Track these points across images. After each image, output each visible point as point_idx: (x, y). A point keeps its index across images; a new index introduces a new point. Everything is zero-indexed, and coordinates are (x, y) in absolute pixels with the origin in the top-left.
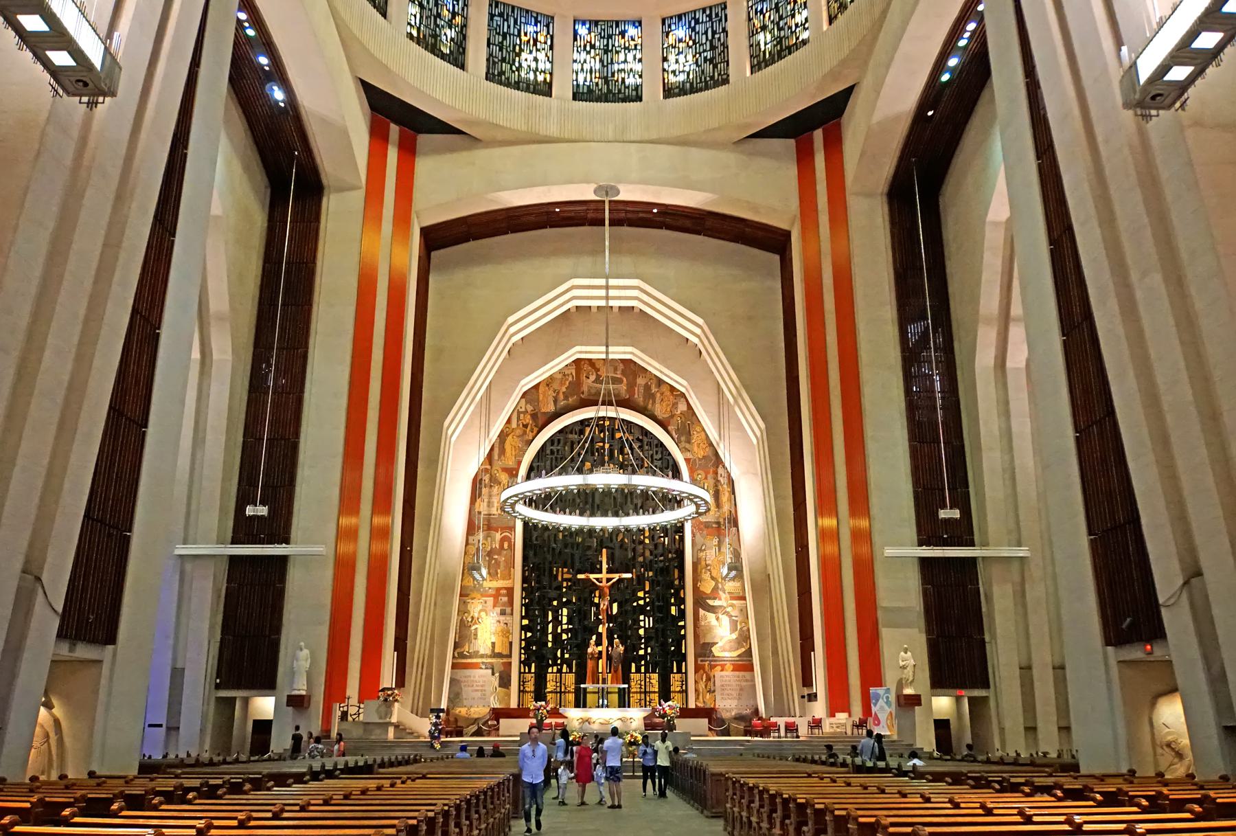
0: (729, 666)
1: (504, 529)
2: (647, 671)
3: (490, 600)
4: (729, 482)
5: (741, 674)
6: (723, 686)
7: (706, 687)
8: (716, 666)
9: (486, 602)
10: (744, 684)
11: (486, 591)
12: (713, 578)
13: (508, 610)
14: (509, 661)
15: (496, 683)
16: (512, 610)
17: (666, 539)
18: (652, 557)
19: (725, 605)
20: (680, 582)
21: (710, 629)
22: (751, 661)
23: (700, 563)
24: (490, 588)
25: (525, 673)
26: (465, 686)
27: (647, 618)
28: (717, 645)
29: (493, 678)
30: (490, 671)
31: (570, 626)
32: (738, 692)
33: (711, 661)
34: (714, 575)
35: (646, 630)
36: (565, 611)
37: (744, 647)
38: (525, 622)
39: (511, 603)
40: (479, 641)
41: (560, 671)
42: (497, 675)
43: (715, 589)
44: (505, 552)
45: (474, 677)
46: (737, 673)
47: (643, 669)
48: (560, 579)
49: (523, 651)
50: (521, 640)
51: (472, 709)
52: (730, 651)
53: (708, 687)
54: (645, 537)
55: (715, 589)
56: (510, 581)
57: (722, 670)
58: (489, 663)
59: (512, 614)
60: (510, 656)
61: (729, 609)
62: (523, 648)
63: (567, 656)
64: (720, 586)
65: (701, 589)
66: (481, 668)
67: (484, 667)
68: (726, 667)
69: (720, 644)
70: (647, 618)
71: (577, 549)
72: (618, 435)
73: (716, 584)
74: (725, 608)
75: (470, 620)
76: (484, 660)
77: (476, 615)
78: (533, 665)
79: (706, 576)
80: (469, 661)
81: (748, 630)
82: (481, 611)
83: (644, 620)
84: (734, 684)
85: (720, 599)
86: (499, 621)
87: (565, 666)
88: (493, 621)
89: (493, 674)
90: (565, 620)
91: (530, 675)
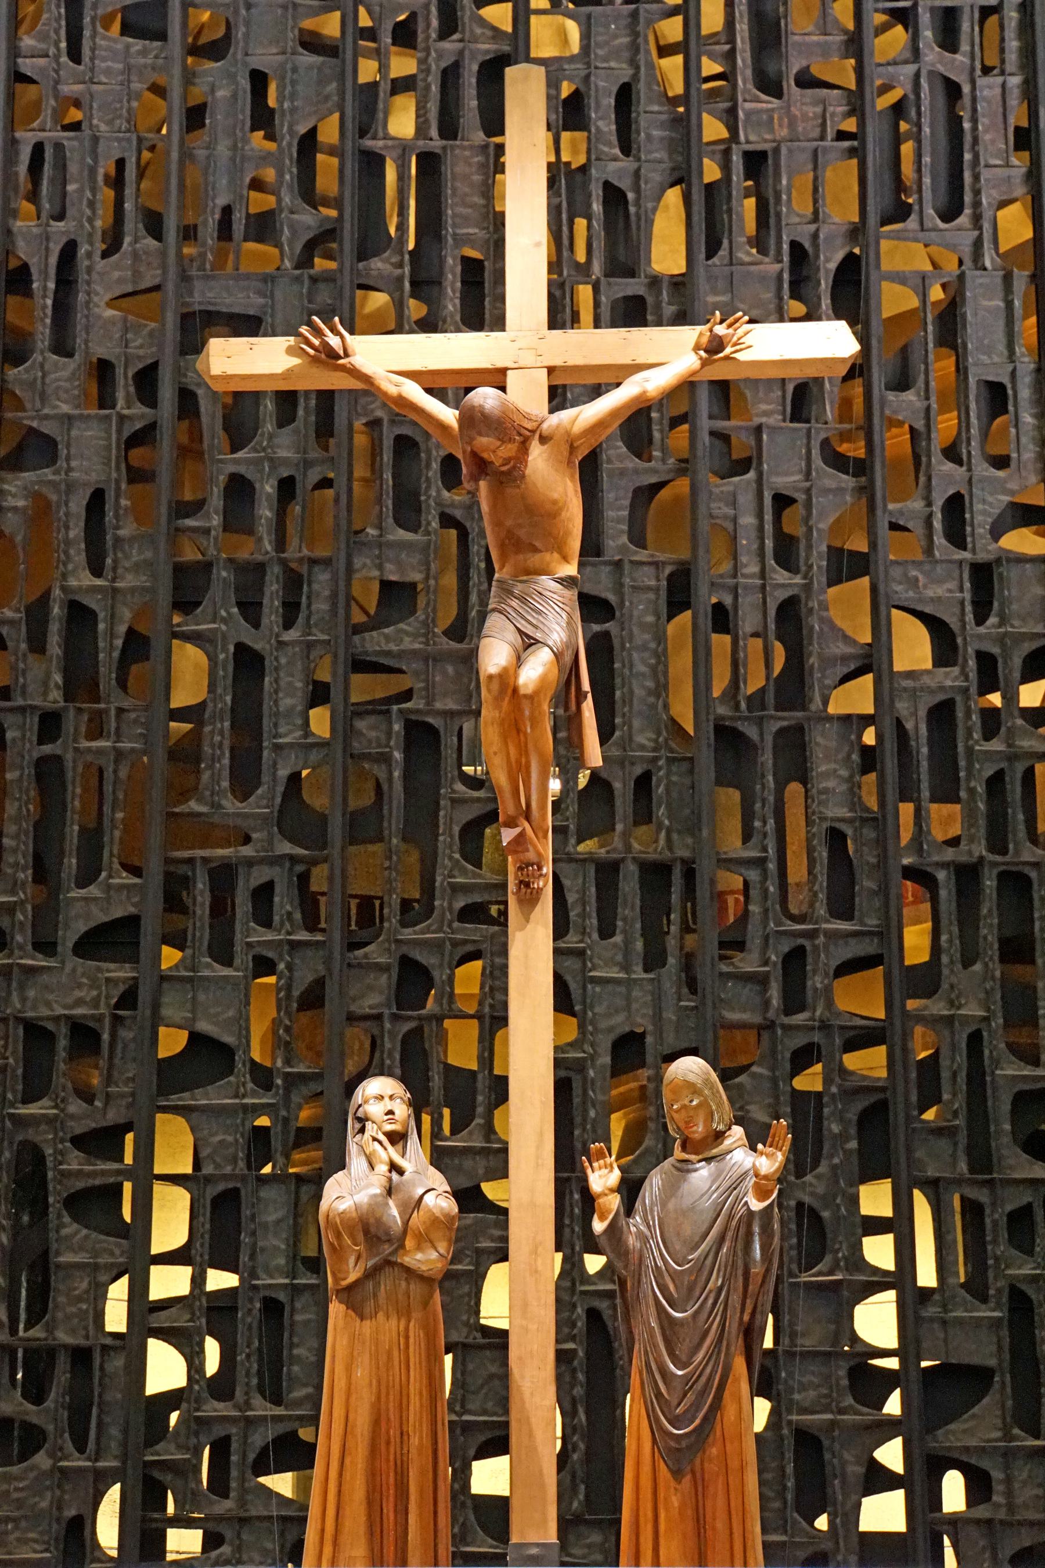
18: (950, 678)
31: (219, 1280)
71: (291, 612)
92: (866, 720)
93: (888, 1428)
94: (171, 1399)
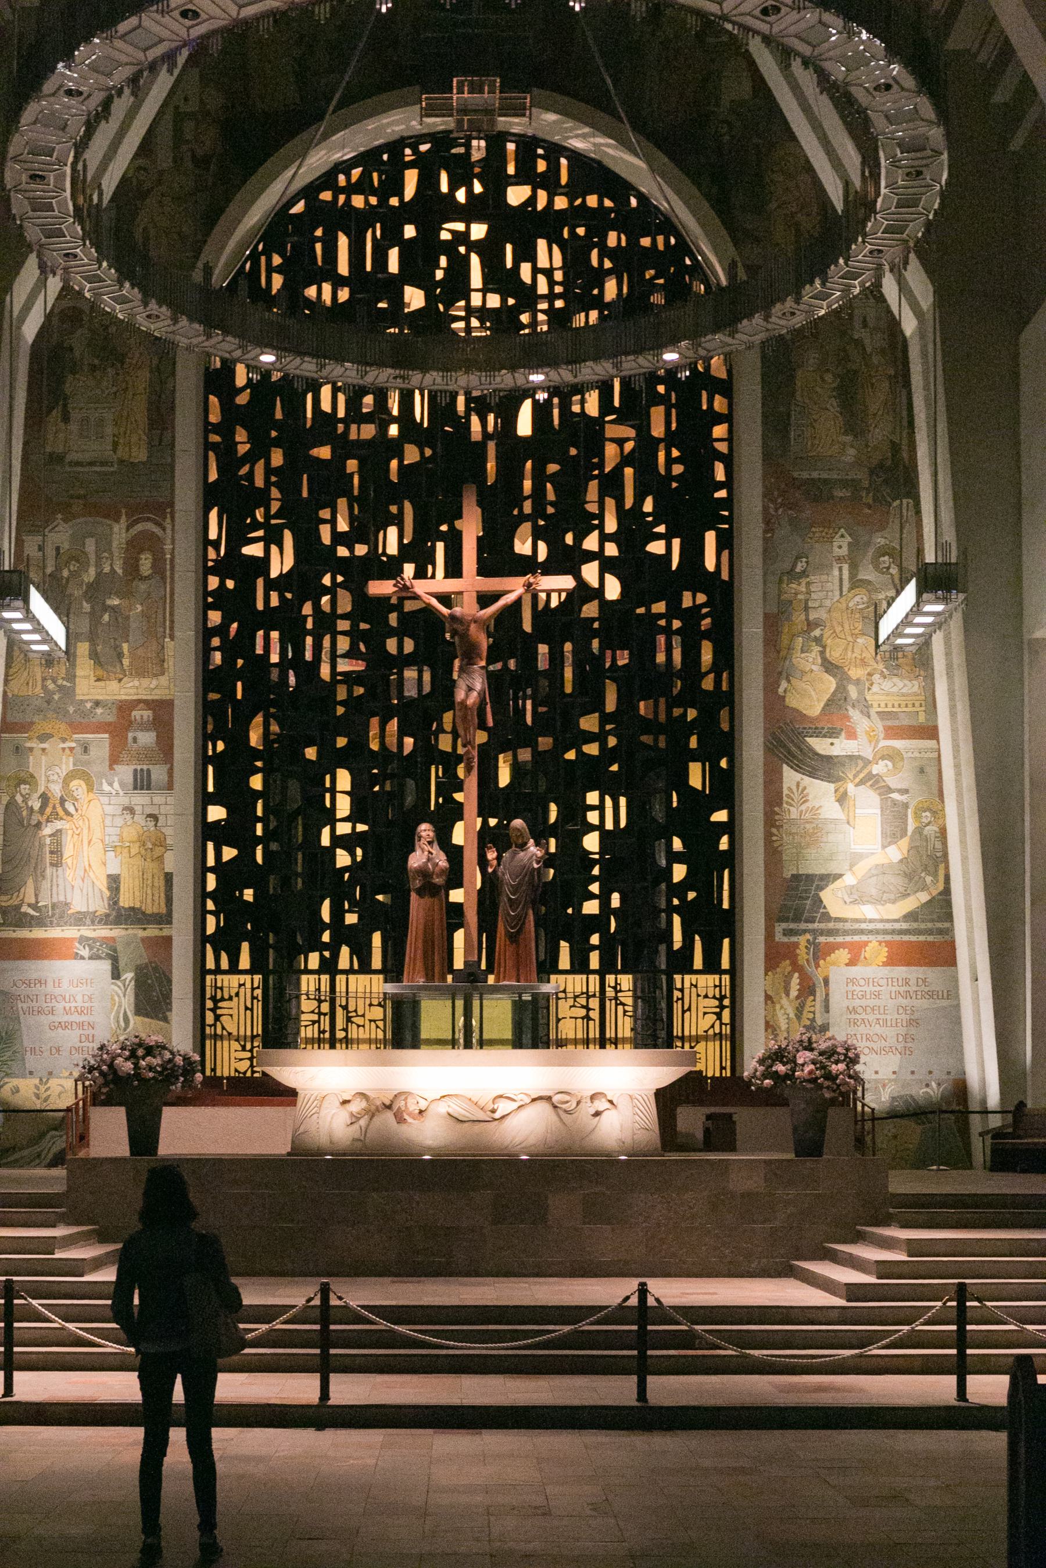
0: (876, 950)
1: (137, 512)
2: (607, 967)
3: (101, 743)
4: (893, 345)
5: (914, 973)
6: (854, 1010)
7: (799, 1011)
8: (832, 948)
9: (86, 750)
10: (923, 1003)
11: (84, 714)
12: (829, 667)
13: (159, 773)
14: (165, 933)
15: (127, 1002)
16: (170, 773)
17: (676, 543)
19: (868, 753)
20: (718, 682)
21: (814, 833)
22: (949, 931)
23: (788, 619)
24: (97, 703)
25: (218, 971)
26: (30, 1011)
27: (608, 799)
28: (838, 883)
29: (116, 988)
30: (106, 966)
31: (361, 828)
32: (902, 1031)
33: (813, 932)
34: (834, 654)
35: (605, 837)
36: (344, 779)
37: (924, 888)
38: (216, 813)
39: (165, 750)
40: (69, 874)
41: (329, 967)
42: (129, 976)
43: (837, 702)
44: (143, 586)
45: (58, 983)
46: (901, 971)
47: (594, 960)
48: (325, 671)
49: (210, 905)
50: (205, 870)
51: (53, 1083)
52: (877, 901)
53: (806, 1015)
54: (604, 538)
55: (837, 702)
56: (163, 680)
57: (852, 963)
58: (105, 940)
59: (170, 786)
60: (165, 919)
61: (876, 769)
62: (212, 895)
63: (351, 919)
64: (853, 692)
65: (793, 701)
66: (77, 957)
67: (85, 952)
68: (868, 952)
69: (849, 880)
70: (608, 799)
72: (516, 195)
73: (841, 688)
74: (867, 762)
75: (37, 805)
76: (87, 932)
77: (56, 790)
78: (245, 946)
79: (808, 661)
80: (38, 933)
81: (943, 832)
82: (70, 777)
83: (601, 808)
84: (891, 1003)
85: (852, 735)
86: (130, 810)
87: (345, 951)
88: (109, 809)
89: (116, 974)
90: (343, 806)
91: (234, 980)
92: (593, 620)
93: (595, 879)
94: (345, 869)
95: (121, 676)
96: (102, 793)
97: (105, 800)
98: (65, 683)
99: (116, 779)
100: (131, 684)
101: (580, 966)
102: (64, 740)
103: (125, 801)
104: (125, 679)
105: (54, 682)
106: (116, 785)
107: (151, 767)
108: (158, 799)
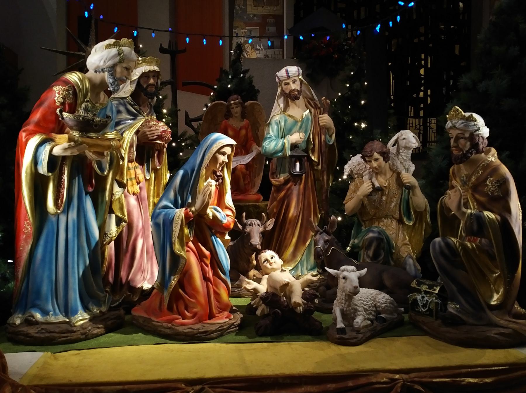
24: (255, 15)
83: (426, 60)
95: (263, 5)
96: (256, 49)
97: (258, 52)
98: (243, 7)
99: (262, 44)
100: (267, 8)
101: (417, 116)
102: (243, 29)
103: (265, 52)
104: (265, 6)
105: (239, 7)
106: (262, 46)
107: (274, 40)
108: (277, 52)
